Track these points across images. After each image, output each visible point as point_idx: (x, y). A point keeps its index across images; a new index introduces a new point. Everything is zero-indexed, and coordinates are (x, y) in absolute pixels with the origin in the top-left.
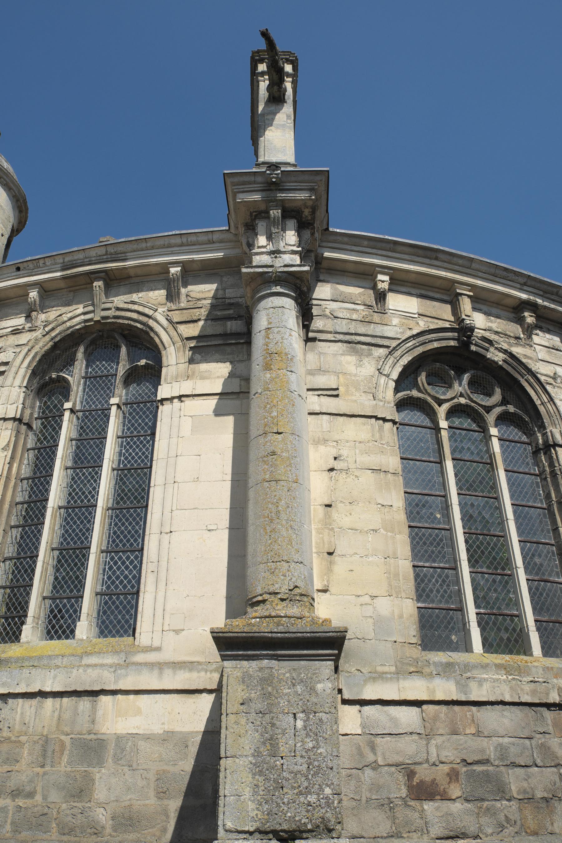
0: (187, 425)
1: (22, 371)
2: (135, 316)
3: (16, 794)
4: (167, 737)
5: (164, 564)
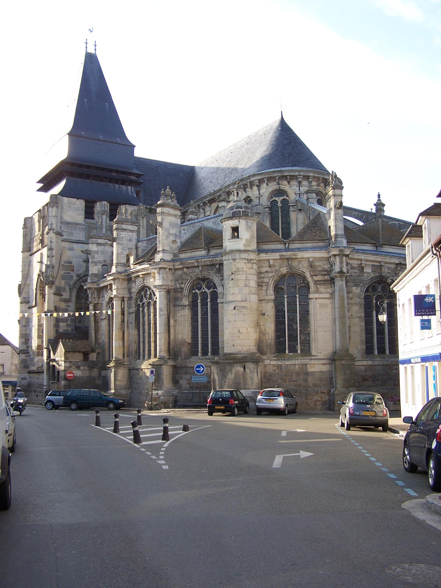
0: (318, 305)
1: (272, 286)
2: (301, 272)
3: (294, 381)
4: (321, 372)
5: (316, 338)
